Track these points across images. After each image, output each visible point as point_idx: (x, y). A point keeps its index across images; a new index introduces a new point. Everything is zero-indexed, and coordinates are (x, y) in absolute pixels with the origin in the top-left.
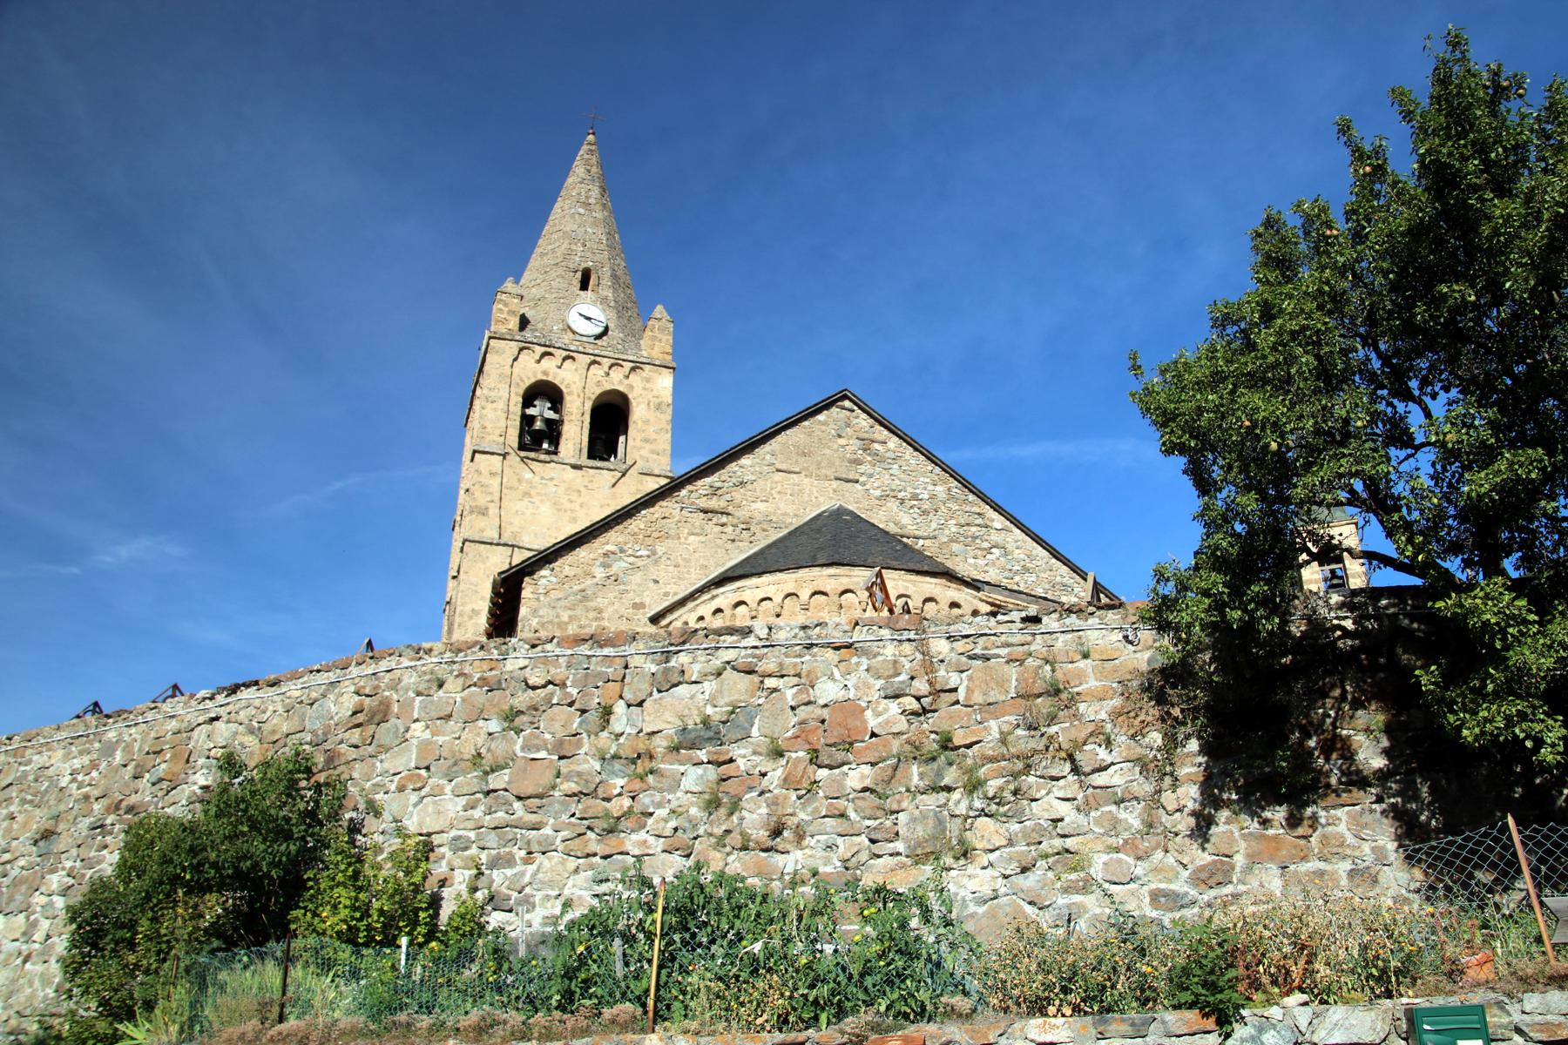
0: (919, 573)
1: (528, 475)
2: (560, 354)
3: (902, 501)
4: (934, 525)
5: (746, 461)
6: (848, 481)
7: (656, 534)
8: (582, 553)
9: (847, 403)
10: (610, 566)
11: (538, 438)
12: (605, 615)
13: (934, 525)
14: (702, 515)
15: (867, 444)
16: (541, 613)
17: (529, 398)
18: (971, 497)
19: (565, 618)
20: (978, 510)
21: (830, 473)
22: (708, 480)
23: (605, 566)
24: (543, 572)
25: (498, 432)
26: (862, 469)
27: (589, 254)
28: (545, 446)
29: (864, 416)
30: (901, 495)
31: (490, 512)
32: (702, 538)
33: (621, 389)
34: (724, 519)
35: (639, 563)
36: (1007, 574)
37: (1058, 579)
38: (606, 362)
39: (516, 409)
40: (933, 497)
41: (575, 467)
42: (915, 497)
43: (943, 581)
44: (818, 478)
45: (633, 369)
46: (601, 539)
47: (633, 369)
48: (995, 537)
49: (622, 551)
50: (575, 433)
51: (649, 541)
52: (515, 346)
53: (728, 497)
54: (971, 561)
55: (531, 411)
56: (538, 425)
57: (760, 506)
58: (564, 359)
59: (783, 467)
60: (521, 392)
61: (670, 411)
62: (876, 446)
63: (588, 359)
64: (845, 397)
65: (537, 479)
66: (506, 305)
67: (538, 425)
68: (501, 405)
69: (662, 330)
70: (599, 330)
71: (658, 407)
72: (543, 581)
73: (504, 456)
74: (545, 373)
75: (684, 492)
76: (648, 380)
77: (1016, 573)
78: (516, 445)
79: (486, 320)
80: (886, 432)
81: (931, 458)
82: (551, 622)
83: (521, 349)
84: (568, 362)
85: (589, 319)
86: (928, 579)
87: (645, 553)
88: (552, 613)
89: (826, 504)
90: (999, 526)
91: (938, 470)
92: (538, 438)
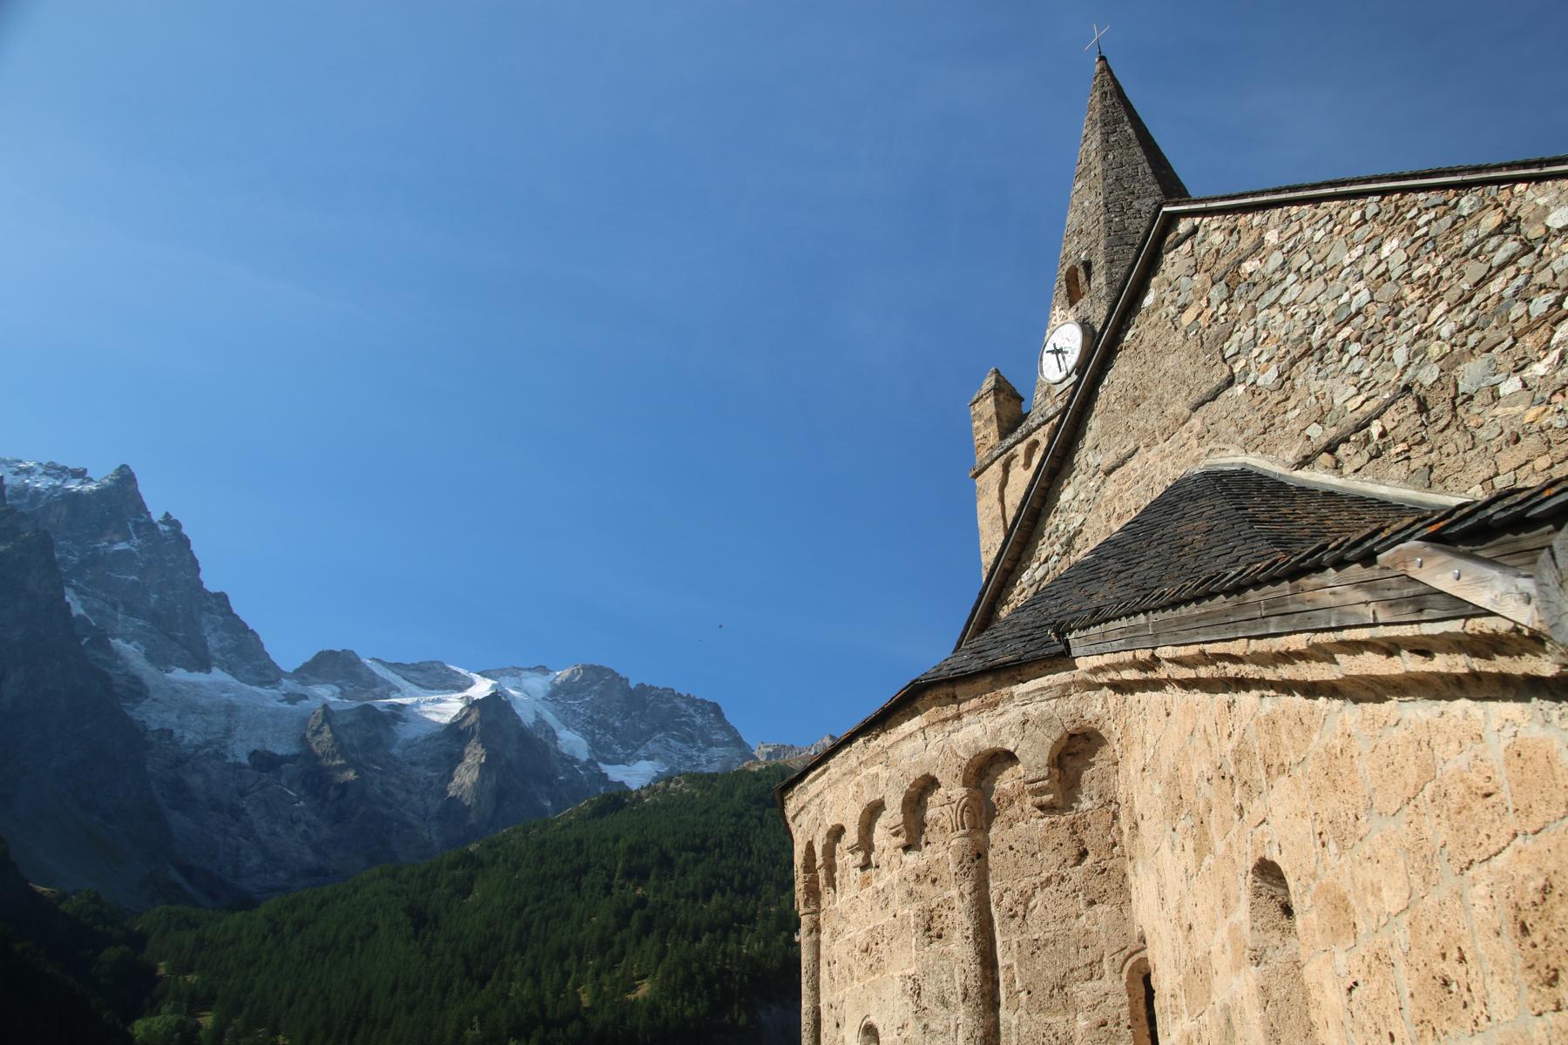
3: (1323, 347)
4: (1400, 356)
6: (1214, 396)
9: (1184, 226)
13: (1400, 356)
15: (1231, 281)
18: (1467, 203)
20: (1492, 220)
21: (1180, 407)
44: (1168, 434)
52: (997, 467)
54: (1510, 386)
62: (1248, 267)
83: (1006, 469)
91: (1372, 205)
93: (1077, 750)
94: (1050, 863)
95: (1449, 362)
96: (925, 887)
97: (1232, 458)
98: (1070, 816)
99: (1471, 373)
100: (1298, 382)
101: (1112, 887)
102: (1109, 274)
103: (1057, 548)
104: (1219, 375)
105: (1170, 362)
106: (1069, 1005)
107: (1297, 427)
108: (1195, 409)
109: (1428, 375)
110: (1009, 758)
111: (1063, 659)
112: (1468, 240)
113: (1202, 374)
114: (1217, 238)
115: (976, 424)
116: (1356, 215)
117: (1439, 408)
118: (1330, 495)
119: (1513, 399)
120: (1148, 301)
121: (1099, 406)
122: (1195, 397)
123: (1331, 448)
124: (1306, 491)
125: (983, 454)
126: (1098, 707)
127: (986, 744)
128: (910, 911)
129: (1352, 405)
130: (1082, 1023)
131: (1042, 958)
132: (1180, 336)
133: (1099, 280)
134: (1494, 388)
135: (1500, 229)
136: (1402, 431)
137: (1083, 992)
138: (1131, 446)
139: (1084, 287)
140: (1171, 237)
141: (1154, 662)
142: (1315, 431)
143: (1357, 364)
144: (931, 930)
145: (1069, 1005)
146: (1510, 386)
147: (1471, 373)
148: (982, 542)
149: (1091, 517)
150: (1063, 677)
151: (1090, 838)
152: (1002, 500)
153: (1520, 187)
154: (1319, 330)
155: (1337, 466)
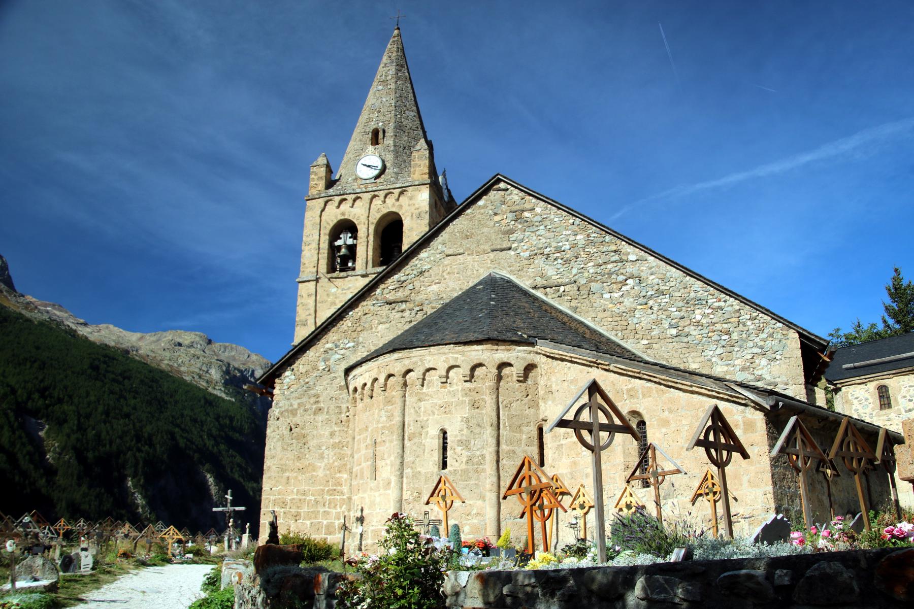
0: (466, 343)
1: (334, 290)
2: (350, 198)
3: (548, 256)
4: (575, 271)
5: (423, 254)
6: (502, 250)
7: (359, 329)
8: (311, 354)
9: (502, 185)
10: (329, 360)
11: (340, 261)
12: (321, 399)
13: (575, 271)
14: (388, 306)
15: (518, 216)
16: (280, 405)
17: (335, 233)
18: (608, 238)
19: (296, 406)
20: (613, 248)
21: (487, 247)
22: (396, 277)
23: (325, 360)
24: (288, 373)
25: (312, 265)
26: (513, 237)
27: (381, 118)
28: (350, 264)
29: (516, 191)
30: (546, 251)
31: (309, 322)
32: (387, 325)
33: (394, 210)
34: (403, 306)
35: (347, 353)
36: (642, 300)
37: (692, 295)
38: (382, 194)
39: (325, 245)
40: (574, 246)
41: (363, 276)
42: (559, 250)
43: (489, 346)
45: (401, 193)
46: (323, 341)
47: (401, 193)
48: (630, 269)
49: (337, 346)
50: (365, 249)
51: (355, 335)
52: (321, 201)
53: (411, 287)
54: (607, 296)
55: (339, 243)
56: (343, 251)
57: (435, 288)
58: (354, 201)
59: (450, 252)
60: (328, 231)
61: (427, 216)
62: (526, 214)
63: (369, 195)
64: (499, 181)
65: (340, 290)
66: (316, 174)
67: (343, 251)
68: (315, 245)
69: (420, 158)
70: (376, 172)
71: (419, 216)
72: (287, 380)
73: (317, 280)
74: (343, 214)
75: (378, 291)
76: (411, 198)
77: (650, 298)
78: (325, 271)
79: (307, 187)
80: (534, 200)
81: (571, 212)
82: (287, 410)
83: (326, 203)
84: (358, 201)
85: (369, 166)
86: (475, 347)
87: (351, 344)
88: (287, 403)
89: (483, 274)
90: (632, 257)
91: (578, 221)
92: (340, 261)
93: (530, 368)
94: (519, 395)
95: (590, 280)
96: (474, 393)
97: (505, 274)
98: (525, 385)
99: (594, 286)
100: (536, 262)
101: (535, 405)
102: (395, 142)
103: (415, 272)
104: (505, 245)
105: (485, 230)
106: (521, 432)
107: (532, 275)
108: (493, 251)
109: (583, 281)
110: (510, 365)
111: (532, 344)
112: (605, 249)
113: (499, 241)
114: (516, 198)
115: (312, 176)
116: (571, 221)
117: (584, 292)
118: (543, 302)
119: (606, 300)
120: (481, 203)
121: (448, 229)
122: (494, 247)
123: (545, 288)
124: (536, 299)
125: (313, 192)
126: (540, 360)
127: (505, 360)
128: (467, 399)
129: (554, 277)
130: (524, 437)
131: (514, 419)
132: (492, 223)
133: (389, 141)
134: (602, 295)
135: (615, 251)
136: (571, 293)
137: (525, 429)
138: (462, 251)
139: (380, 141)
140: (496, 187)
141: (639, 373)
142: (538, 279)
143: (559, 266)
144: (475, 405)
145: (521, 432)
146: (607, 296)
147: (594, 286)
148: (305, 231)
149: (435, 268)
150: (530, 349)
151: (530, 392)
152: (321, 216)
153: (623, 243)
154: (548, 249)
155: (546, 294)
